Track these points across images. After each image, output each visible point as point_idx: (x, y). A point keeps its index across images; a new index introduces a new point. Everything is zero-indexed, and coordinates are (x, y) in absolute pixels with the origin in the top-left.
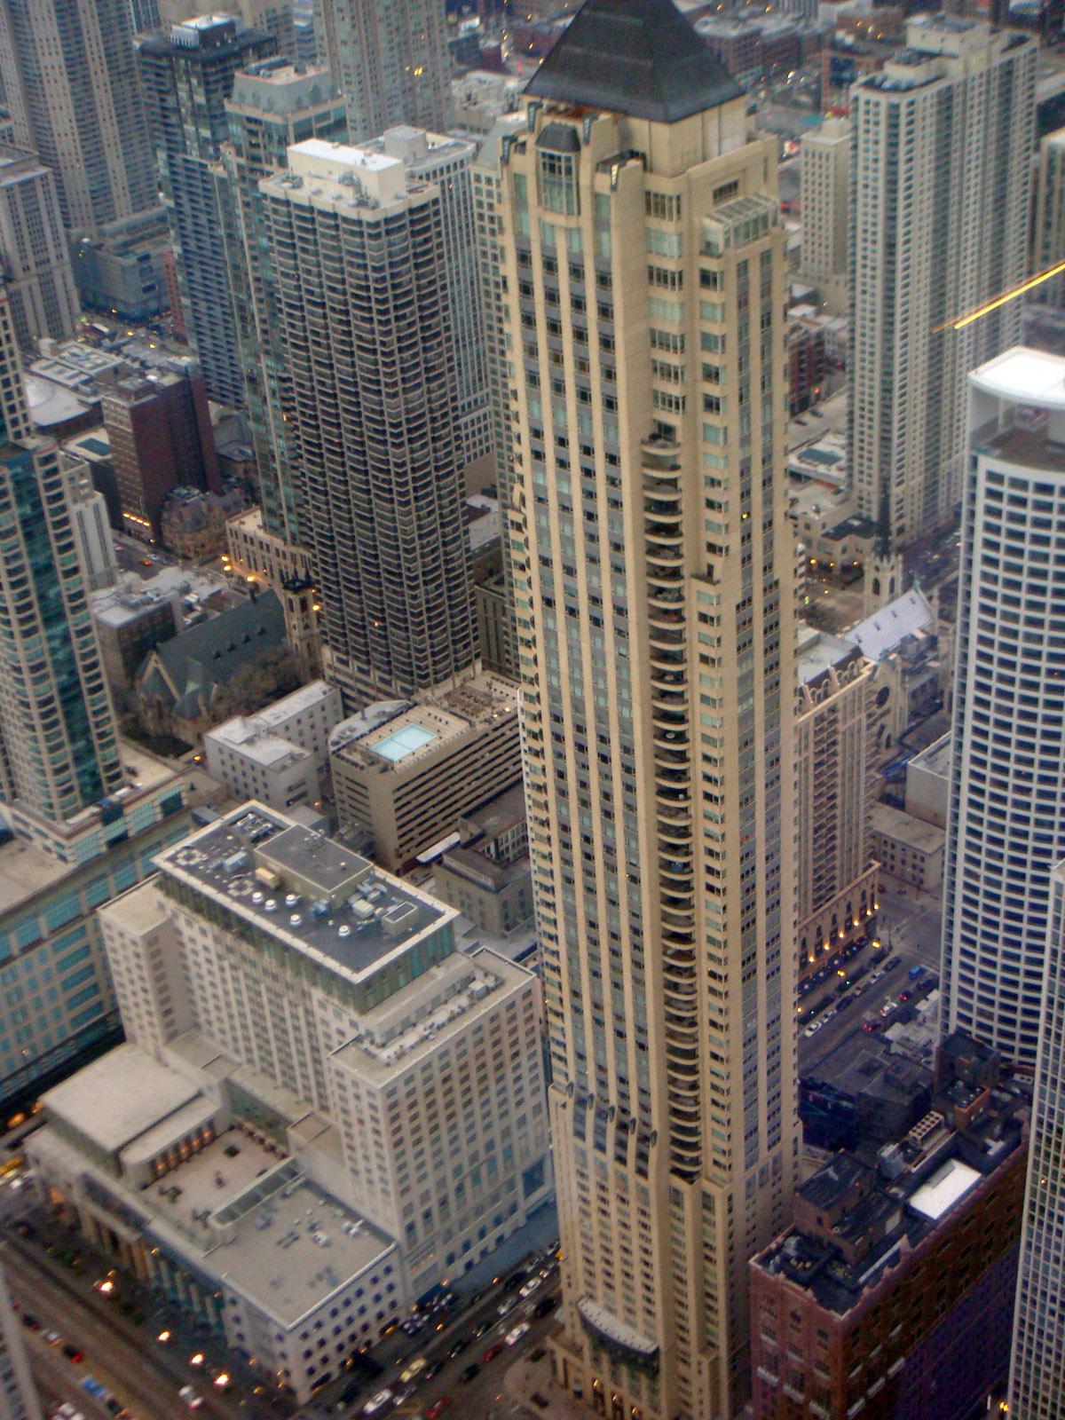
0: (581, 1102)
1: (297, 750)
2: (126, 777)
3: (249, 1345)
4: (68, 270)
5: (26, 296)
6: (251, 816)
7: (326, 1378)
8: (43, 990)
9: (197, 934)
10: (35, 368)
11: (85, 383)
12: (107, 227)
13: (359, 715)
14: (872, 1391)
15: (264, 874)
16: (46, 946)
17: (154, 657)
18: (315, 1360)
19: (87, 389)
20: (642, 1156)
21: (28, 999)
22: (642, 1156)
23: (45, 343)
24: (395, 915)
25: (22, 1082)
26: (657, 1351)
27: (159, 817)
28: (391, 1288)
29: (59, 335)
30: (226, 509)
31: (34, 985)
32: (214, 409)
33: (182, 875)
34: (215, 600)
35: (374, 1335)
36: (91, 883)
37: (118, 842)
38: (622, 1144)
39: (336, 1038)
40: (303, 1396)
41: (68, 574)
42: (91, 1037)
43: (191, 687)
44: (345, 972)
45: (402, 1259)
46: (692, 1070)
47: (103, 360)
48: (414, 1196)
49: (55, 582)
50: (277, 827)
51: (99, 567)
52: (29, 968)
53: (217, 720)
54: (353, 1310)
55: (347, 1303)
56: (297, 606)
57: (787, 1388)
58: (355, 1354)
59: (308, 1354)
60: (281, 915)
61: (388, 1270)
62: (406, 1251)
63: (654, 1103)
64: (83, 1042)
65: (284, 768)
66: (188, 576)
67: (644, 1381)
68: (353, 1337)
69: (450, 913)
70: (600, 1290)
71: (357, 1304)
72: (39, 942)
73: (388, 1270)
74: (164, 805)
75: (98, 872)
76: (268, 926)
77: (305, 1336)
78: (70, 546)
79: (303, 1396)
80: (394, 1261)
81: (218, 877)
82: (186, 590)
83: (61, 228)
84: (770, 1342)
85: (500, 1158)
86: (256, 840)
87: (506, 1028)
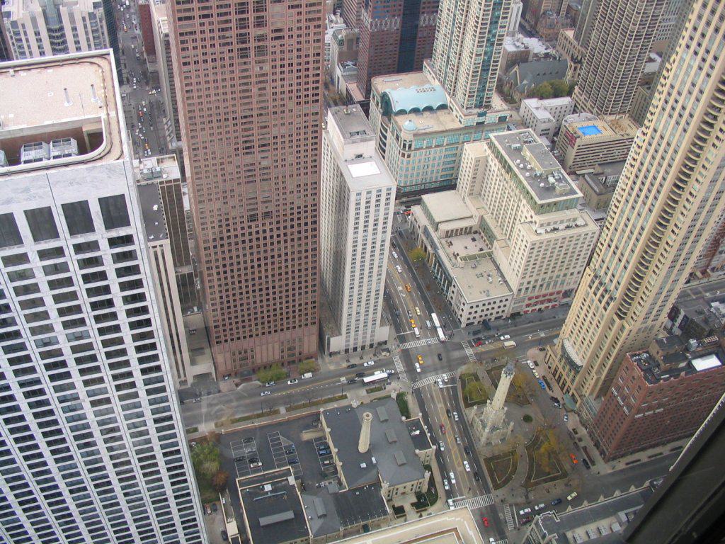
0: (596, 277)
1: (552, 118)
6: (527, 134)
9: (494, 164)
13: (578, 114)
14: (647, 414)
18: (471, 316)
20: (608, 304)
21: (430, 163)
22: (608, 304)
25: (418, 188)
27: (497, 121)
28: (505, 306)
36: (466, 134)
38: (603, 296)
39: (524, 218)
40: (463, 325)
41: (501, 27)
42: (443, 184)
43: (525, 82)
46: (639, 284)
51: (511, 29)
52: (435, 153)
53: (531, 95)
54: (490, 307)
55: (489, 304)
56: (573, 68)
59: (470, 313)
61: (507, 300)
62: (515, 297)
65: (544, 122)
68: (486, 315)
69: (580, 194)
73: (507, 300)
75: (470, 131)
77: (472, 307)
78: (506, 18)
79: (463, 325)
80: (510, 298)
81: (508, 149)
85: (559, 282)
86: (525, 142)
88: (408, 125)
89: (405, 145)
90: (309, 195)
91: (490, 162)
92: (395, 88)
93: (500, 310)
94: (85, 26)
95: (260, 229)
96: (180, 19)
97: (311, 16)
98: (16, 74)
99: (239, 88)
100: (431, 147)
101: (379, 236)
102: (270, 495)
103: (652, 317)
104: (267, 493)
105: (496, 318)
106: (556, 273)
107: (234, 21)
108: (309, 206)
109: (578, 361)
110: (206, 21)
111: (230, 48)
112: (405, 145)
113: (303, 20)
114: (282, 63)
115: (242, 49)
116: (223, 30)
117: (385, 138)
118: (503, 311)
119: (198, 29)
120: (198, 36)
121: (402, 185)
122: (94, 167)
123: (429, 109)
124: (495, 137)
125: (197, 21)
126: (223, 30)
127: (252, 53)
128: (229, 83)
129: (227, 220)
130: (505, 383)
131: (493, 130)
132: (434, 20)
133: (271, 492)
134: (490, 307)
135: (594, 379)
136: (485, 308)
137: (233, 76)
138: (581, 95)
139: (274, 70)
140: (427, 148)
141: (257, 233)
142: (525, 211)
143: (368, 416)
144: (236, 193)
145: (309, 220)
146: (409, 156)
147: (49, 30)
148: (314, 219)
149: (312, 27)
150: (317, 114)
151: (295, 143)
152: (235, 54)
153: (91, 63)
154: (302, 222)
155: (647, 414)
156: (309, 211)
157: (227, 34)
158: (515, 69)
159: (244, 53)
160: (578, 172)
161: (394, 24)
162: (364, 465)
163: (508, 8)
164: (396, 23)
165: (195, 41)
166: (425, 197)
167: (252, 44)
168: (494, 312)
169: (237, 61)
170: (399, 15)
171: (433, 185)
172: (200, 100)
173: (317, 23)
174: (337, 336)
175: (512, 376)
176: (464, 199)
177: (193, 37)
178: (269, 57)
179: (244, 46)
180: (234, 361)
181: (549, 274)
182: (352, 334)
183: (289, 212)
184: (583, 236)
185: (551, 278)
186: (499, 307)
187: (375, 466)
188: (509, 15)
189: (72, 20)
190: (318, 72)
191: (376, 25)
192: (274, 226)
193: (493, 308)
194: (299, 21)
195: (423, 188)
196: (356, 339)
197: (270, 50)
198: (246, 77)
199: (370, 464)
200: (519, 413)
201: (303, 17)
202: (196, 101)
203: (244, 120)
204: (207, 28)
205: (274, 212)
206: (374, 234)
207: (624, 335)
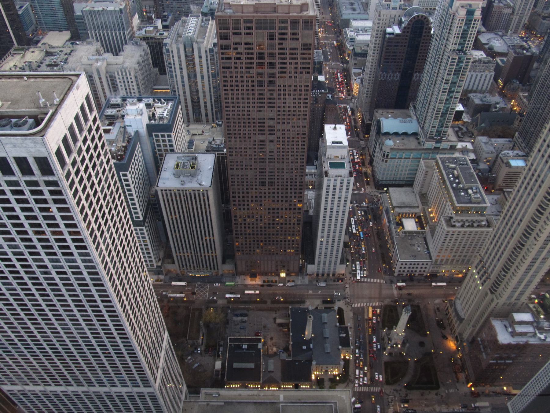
0: (481, 261)
1: (494, 151)
2: (447, 136)
3: (393, 258)
4: (527, 17)
5: (514, 19)
7: (402, 274)
8: (404, 168)
9: (436, 175)
10: (504, 37)
11: (512, 46)
12: (545, 12)
14: (499, 361)
15: (455, 172)
16: (410, 160)
18: (402, 270)
19: (511, 47)
20: (485, 281)
21: (400, 168)
22: (485, 281)
23: (510, 32)
24: (475, 198)
26: (463, 319)
28: (426, 268)
29: (515, 32)
30: (522, 89)
31: (403, 166)
32: (535, 65)
33: (440, 162)
34: (502, 109)
35: (417, 274)
37: (436, 148)
38: (483, 276)
40: (396, 274)
41: (458, 86)
42: (408, 183)
43: (483, 125)
44: (456, 202)
45: (431, 264)
46: (506, 272)
47: (517, 41)
48: (441, 255)
49: (455, 87)
50: (467, 164)
51: (484, 88)
52: (404, 162)
53: (483, 135)
54: (415, 266)
55: (414, 264)
56: (519, 120)
57: (481, 346)
58: (411, 275)
59: (401, 268)
60: (451, 183)
61: (427, 264)
62: (433, 263)
63: (494, 272)
64: (407, 183)
65: (488, 153)
66: (501, 100)
67: (458, 322)
68: (412, 271)
69: (488, 205)
70: (461, 299)
71: (416, 266)
72: (409, 158)
73: (427, 264)
74: (451, 146)
75: (429, 152)
76: (448, 183)
77: (402, 264)
78: (463, 81)
79: (396, 274)
80: (429, 263)
82: (498, 103)
83: (532, 7)
84: (484, 336)
85: (466, 261)
86: (461, 164)
87: (484, 236)
88: (389, 143)
89: (384, 154)
90: (298, 176)
91: (435, 174)
92: (387, 118)
93: (422, 270)
94: (207, 56)
95: (267, 191)
96: (223, 59)
97: (304, 66)
98: (29, 80)
99: (257, 105)
100: (401, 158)
101: (341, 208)
102: (245, 351)
103: (515, 297)
104: (244, 349)
105: (419, 274)
106: (464, 254)
107: (255, 63)
108: (298, 183)
109: (462, 314)
110: (238, 61)
111: (253, 79)
112: (384, 154)
113: (299, 68)
114: (285, 92)
115: (260, 81)
116: (249, 68)
117: (376, 148)
118: (424, 271)
119: (233, 65)
120: (233, 70)
121: (380, 179)
122: (26, 139)
123: (405, 134)
124: (440, 158)
125: (233, 61)
126: (249, 68)
127: (266, 85)
128: (251, 101)
129: (247, 182)
130: (404, 318)
131: (445, 153)
132: (420, 77)
133: (246, 350)
134: (415, 266)
135: (471, 330)
136: (411, 266)
137: (253, 97)
139: (279, 97)
140: (399, 158)
141: (265, 193)
142: (448, 209)
143: (310, 317)
144: (253, 167)
145: (298, 191)
146: (386, 161)
147: (186, 56)
148: (301, 191)
149: (304, 73)
150: (305, 127)
151: (291, 143)
152: (255, 84)
153: (70, 79)
154: (293, 191)
155: (499, 361)
156: (298, 186)
157: (251, 71)
159: (261, 84)
160: (504, 190)
161: (397, 76)
162: (304, 347)
163: (465, 75)
164: (397, 77)
165: (231, 72)
166: (391, 189)
168: (418, 270)
169: (256, 88)
170: (399, 72)
171: (402, 183)
172: (233, 109)
173: (307, 70)
174: (312, 264)
175: (409, 314)
176: (415, 195)
177: (230, 70)
178: (276, 88)
179: (261, 79)
180: (247, 266)
181: (459, 254)
182: (322, 265)
183: (285, 184)
184: (485, 233)
185: (460, 256)
186: (421, 268)
187: (311, 349)
188: (465, 79)
189: (200, 52)
190: (307, 101)
191: (384, 76)
192: (276, 191)
193: (417, 268)
194: (296, 68)
195: (394, 183)
196: (324, 269)
197: (277, 83)
198: (262, 99)
199: (308, 347)
200: (417, 338)
201: (299, 66)
202: (231, 109)
203: (260, 125)
204: (239, 65)
205: (276, 183)
206: (338, 206)
207: (493, 305)
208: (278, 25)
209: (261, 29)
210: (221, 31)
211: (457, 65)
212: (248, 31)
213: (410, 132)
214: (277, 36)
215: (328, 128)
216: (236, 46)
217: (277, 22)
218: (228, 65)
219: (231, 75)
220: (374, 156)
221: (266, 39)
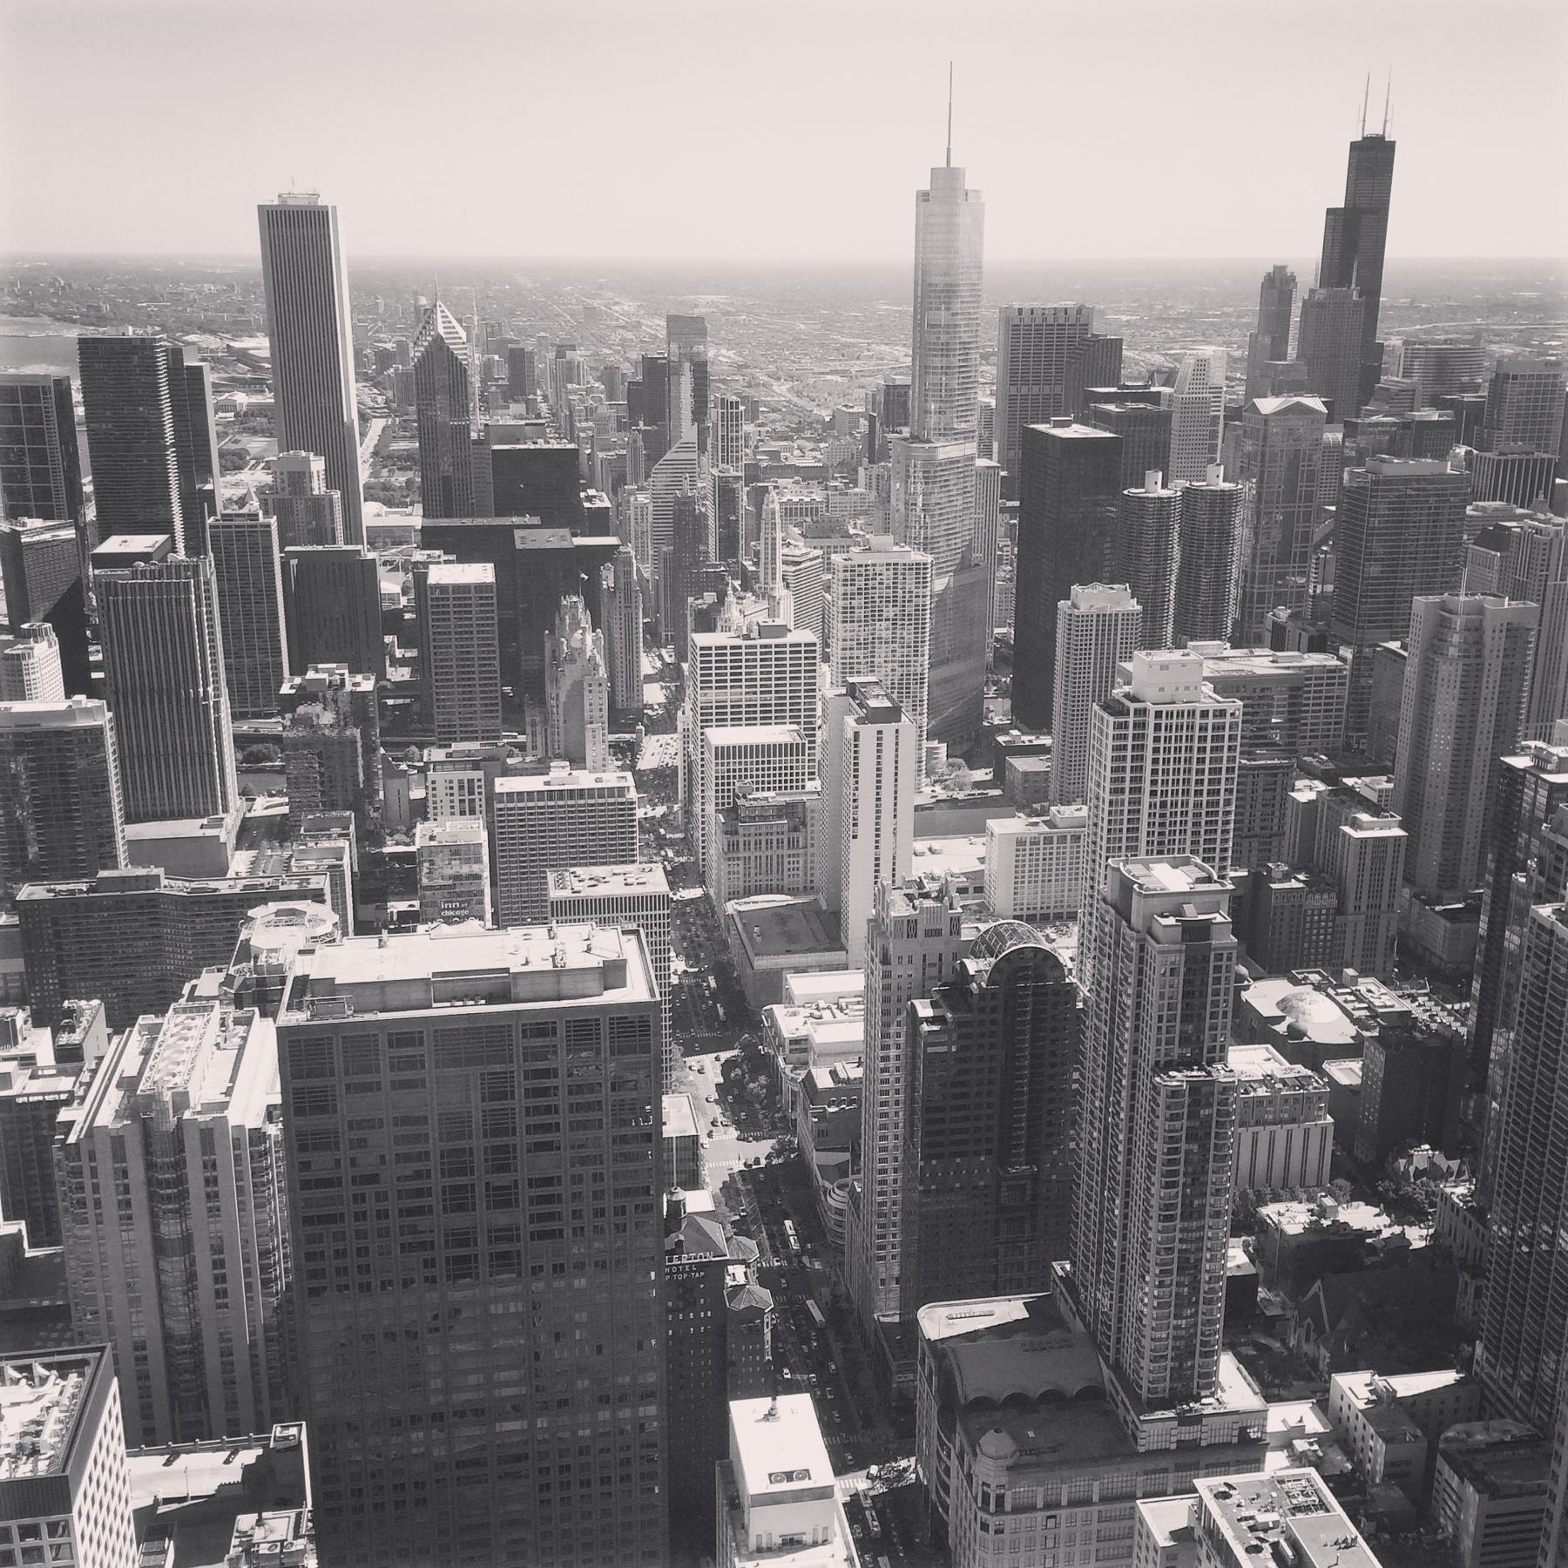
5: (1350, 929)
6: (1303, 1482)
17: (1318, 1283)
27: (1235, 1440)
36: (1154, 1472)
43: (1343, 1324)
50: (1322, 1506)
52: (1071, 1520)
56: (1471, 1291)
72: (1087, 1502)
75: (1163, 1464)
89: (986, 1496)
100: (1058, 1506)
110: (369, 1190)
112: (986, 1496)
116: (411, 1212)
117: (947, 1470)
123: (1055, 1398)
126: (411, 1212)
131: (1227, 1464)
138: (1493, 1367)
147: (150, 1166)
157: (423, 1222)
158: (1314, 1289)
167: (483, 1247)
170: (989, 1152)
177: (334, 1227)
179: (462, 1251)
208: (519, 1044)
209: (456, 1062)
210: (299, 1083)
211: (1192, 1115)
212: (408, 1075)
213: (1073, 1386)
214: (520, 1084)
215: (744, 1413)
216: (359, 1134)
217: (517, 1034)
218: (326, 1211)
219: (340, 1246)
220: (946, 1509)
221: (475, 1097)
